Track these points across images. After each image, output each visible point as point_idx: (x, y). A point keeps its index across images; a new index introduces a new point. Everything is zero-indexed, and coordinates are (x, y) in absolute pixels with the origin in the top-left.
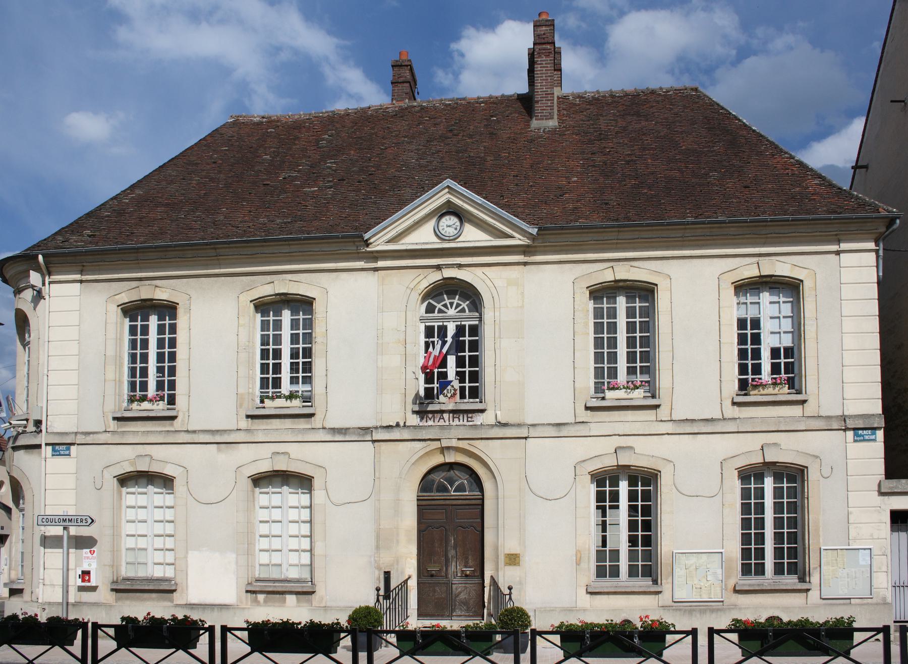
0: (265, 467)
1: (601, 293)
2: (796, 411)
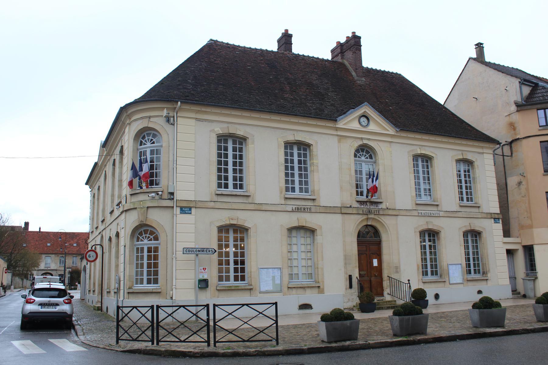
0: (296, 224)
2: (476, 210)
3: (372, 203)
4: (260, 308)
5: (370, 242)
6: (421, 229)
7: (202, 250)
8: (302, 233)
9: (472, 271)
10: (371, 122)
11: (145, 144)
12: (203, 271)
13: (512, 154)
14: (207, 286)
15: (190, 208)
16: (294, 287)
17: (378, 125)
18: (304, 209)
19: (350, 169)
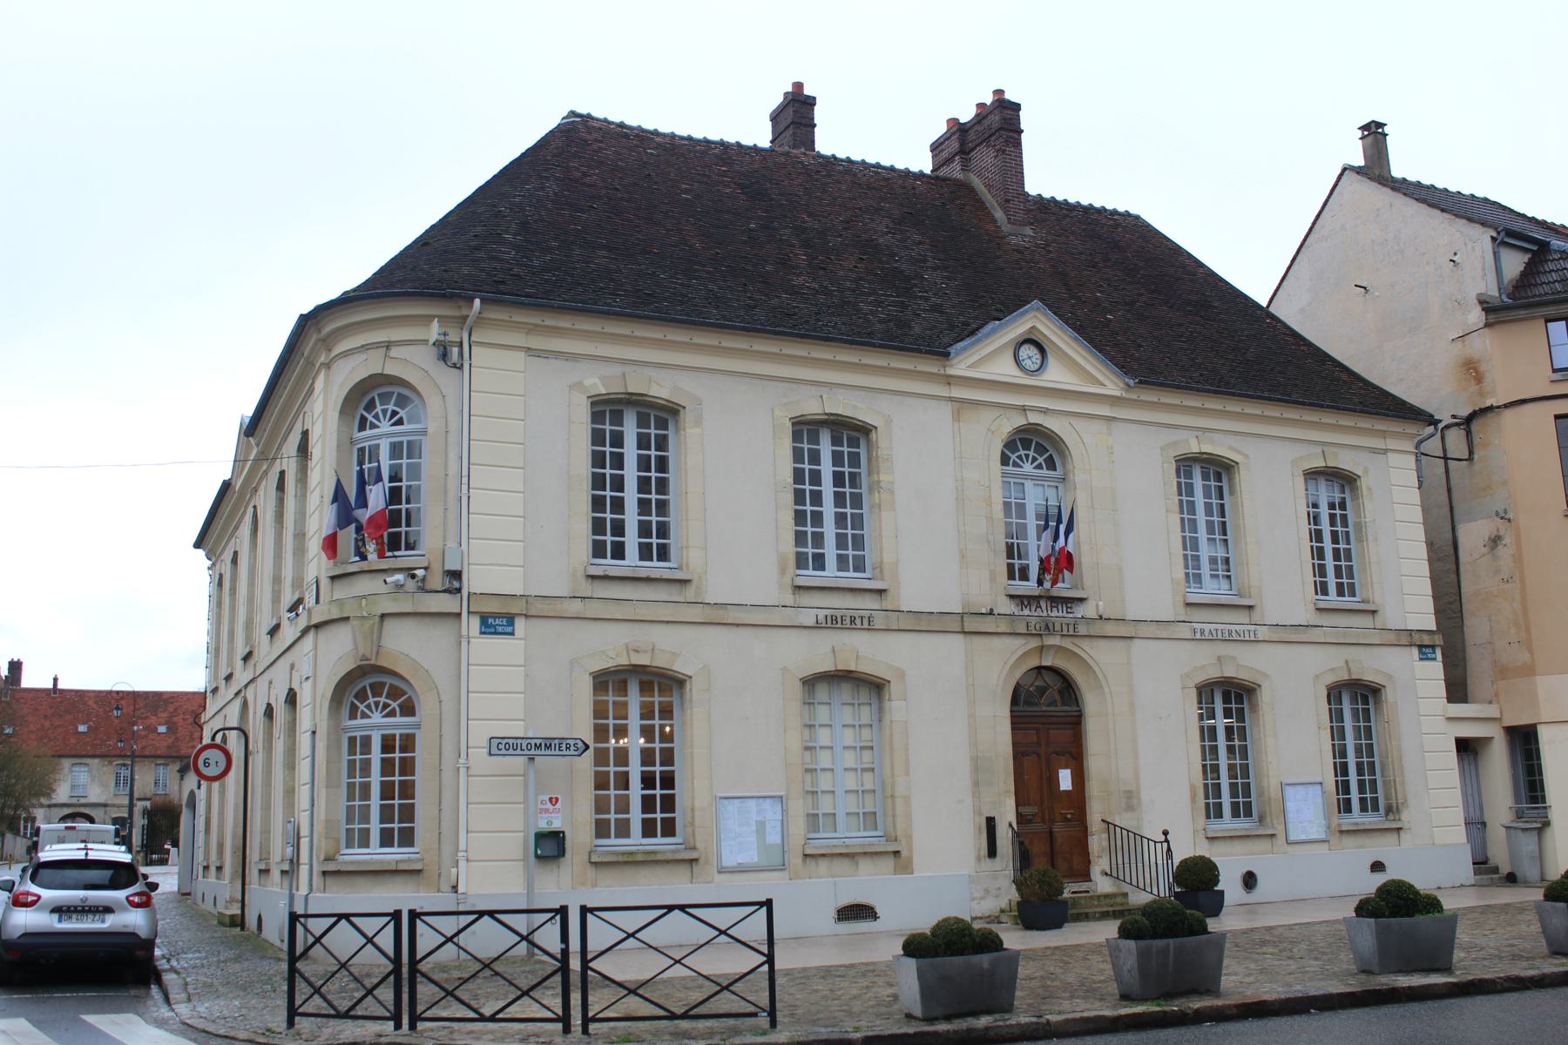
0: (827, 666)
2: (1366, 621)
3: (1056, 601)
4: (722, 918)
5: (1048, 719)
6: (1201, 678)
7: (547, 744)
8: (846, 691)
9: (1355, 805)
10: (1051, 360)
11: (373, 426)
12: (549, 806)
13: (1471, 452)
14: (561, 852)
15: (511, 619)
16: (823, 855)
17: (1074, 367)
19: (989, 502)
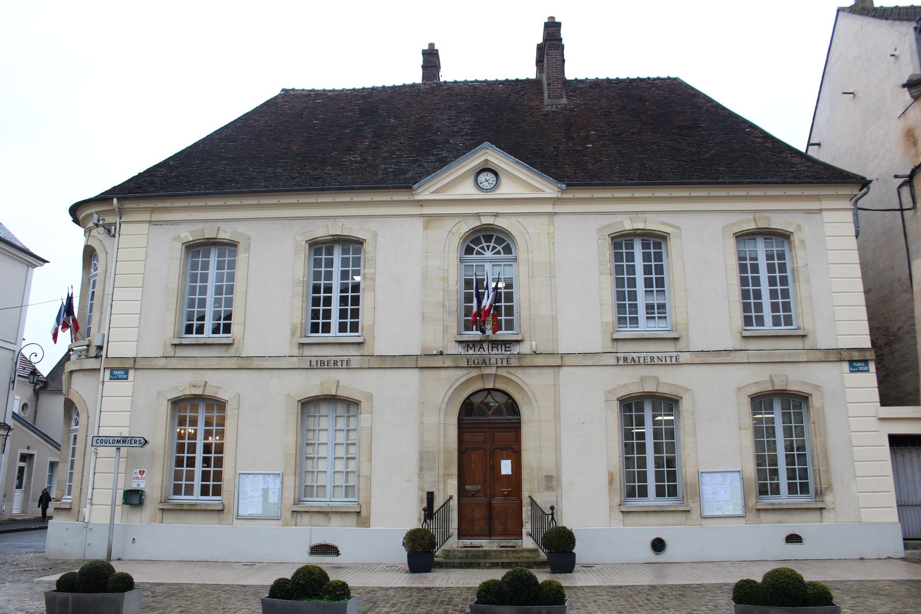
1: (621, 242)
2: (798, 344)
3: (495, 343)
5: (488, 428)
7: (124, 440)
8: (324, 409)
10: (504, 180)
12: (139, 475)
13: (914, 202)
14: (141, 503)
15: (126, 371)
16: (306, 512)
17: (518, 181)
18: (335, 363)
19: (445, 279)
